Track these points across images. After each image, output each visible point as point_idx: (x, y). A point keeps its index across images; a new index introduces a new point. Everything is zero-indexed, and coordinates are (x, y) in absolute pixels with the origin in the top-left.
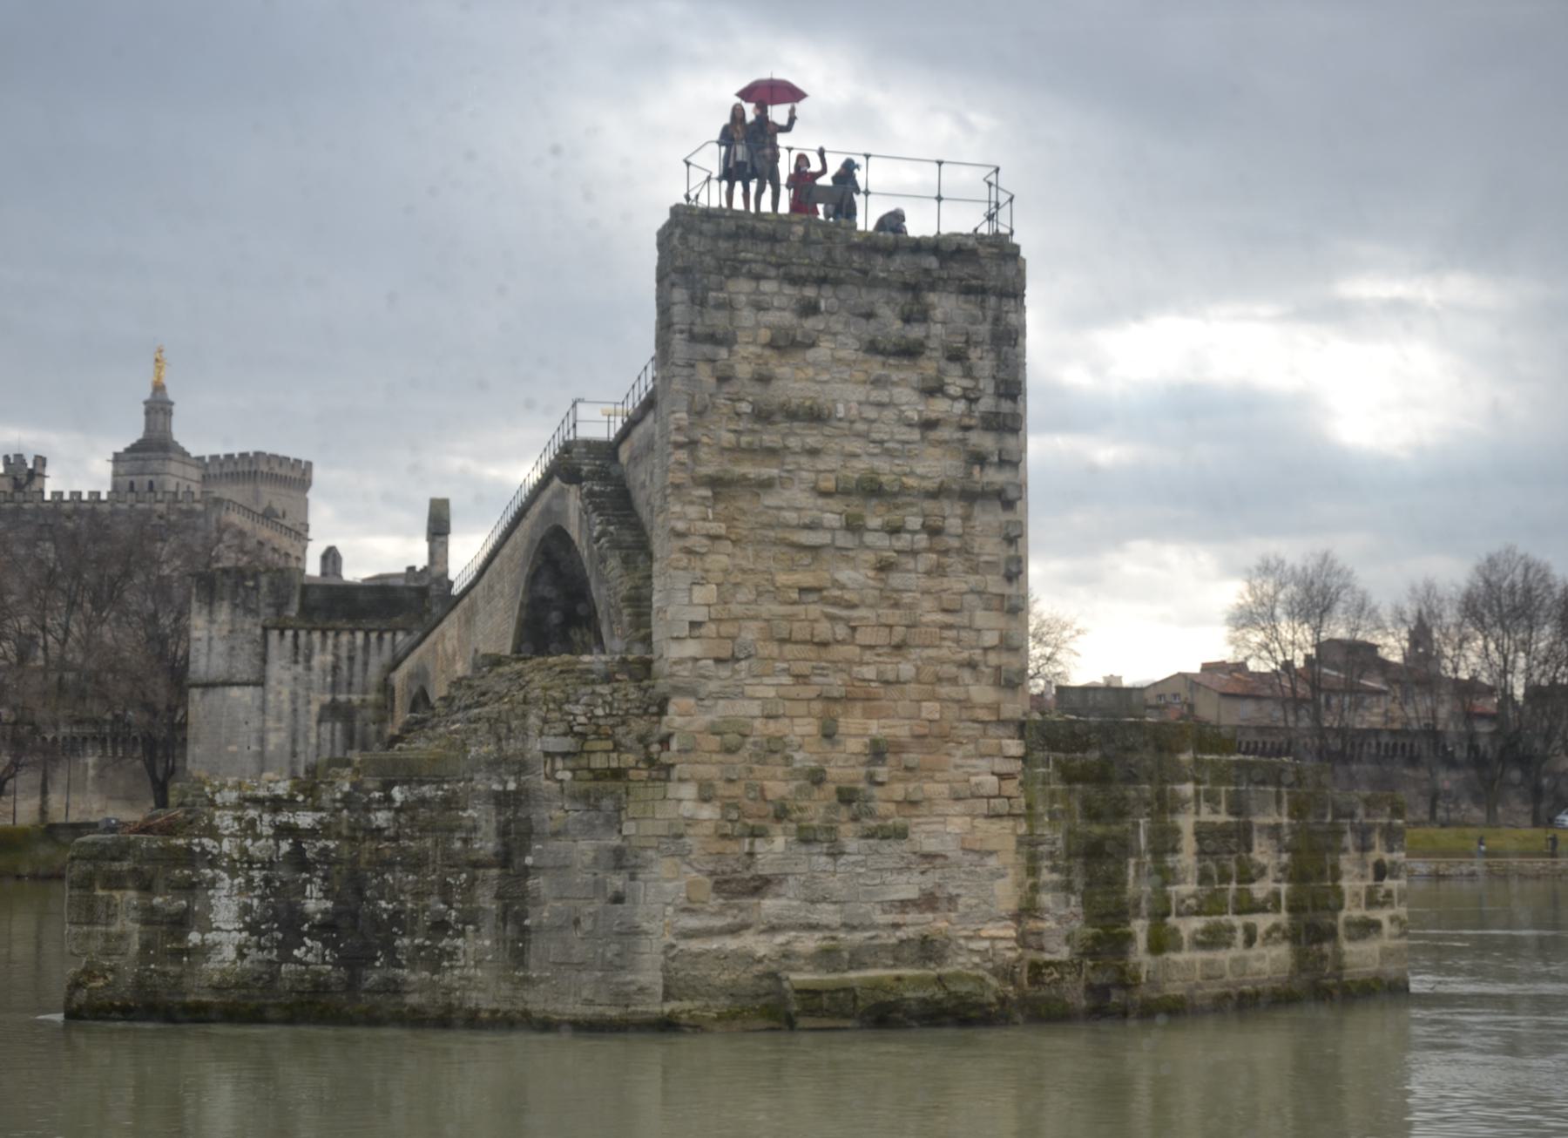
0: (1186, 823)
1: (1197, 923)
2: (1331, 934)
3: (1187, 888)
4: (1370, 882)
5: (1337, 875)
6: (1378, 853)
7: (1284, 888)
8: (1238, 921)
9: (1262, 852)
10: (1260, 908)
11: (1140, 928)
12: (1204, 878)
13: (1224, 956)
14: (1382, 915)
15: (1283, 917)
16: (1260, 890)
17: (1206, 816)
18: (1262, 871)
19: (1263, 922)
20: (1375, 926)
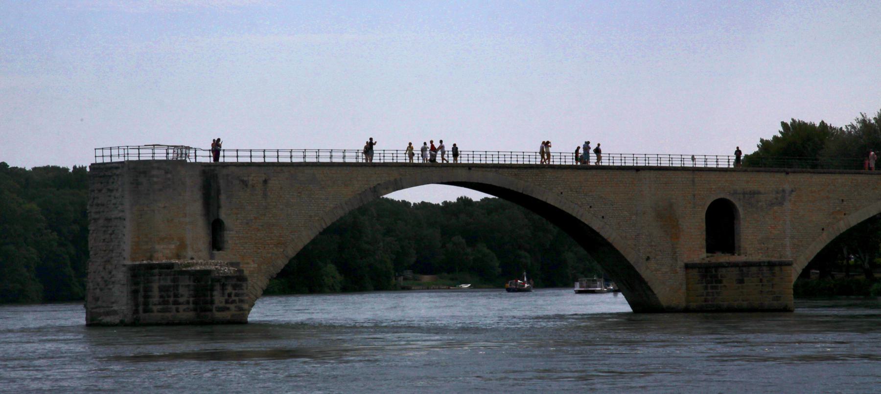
0: (155, 286)
1: (159, 307)
2: (211, 310)
3: (156, 299)
4: (226, 297)
5: (212, 296)
6: (229, 289)
7: (191, 299)
8: (174, 307)
9: (182, 290)
10: (182, 304)
11: (141, 308)
12: (161, 297)
13: (168, 314)
14: (232, 306)
15: (191, 306)
16: (181, 300)
17: (163, 283)
18: (182, 296)
19: (182, 307)
20: (228, 309)
